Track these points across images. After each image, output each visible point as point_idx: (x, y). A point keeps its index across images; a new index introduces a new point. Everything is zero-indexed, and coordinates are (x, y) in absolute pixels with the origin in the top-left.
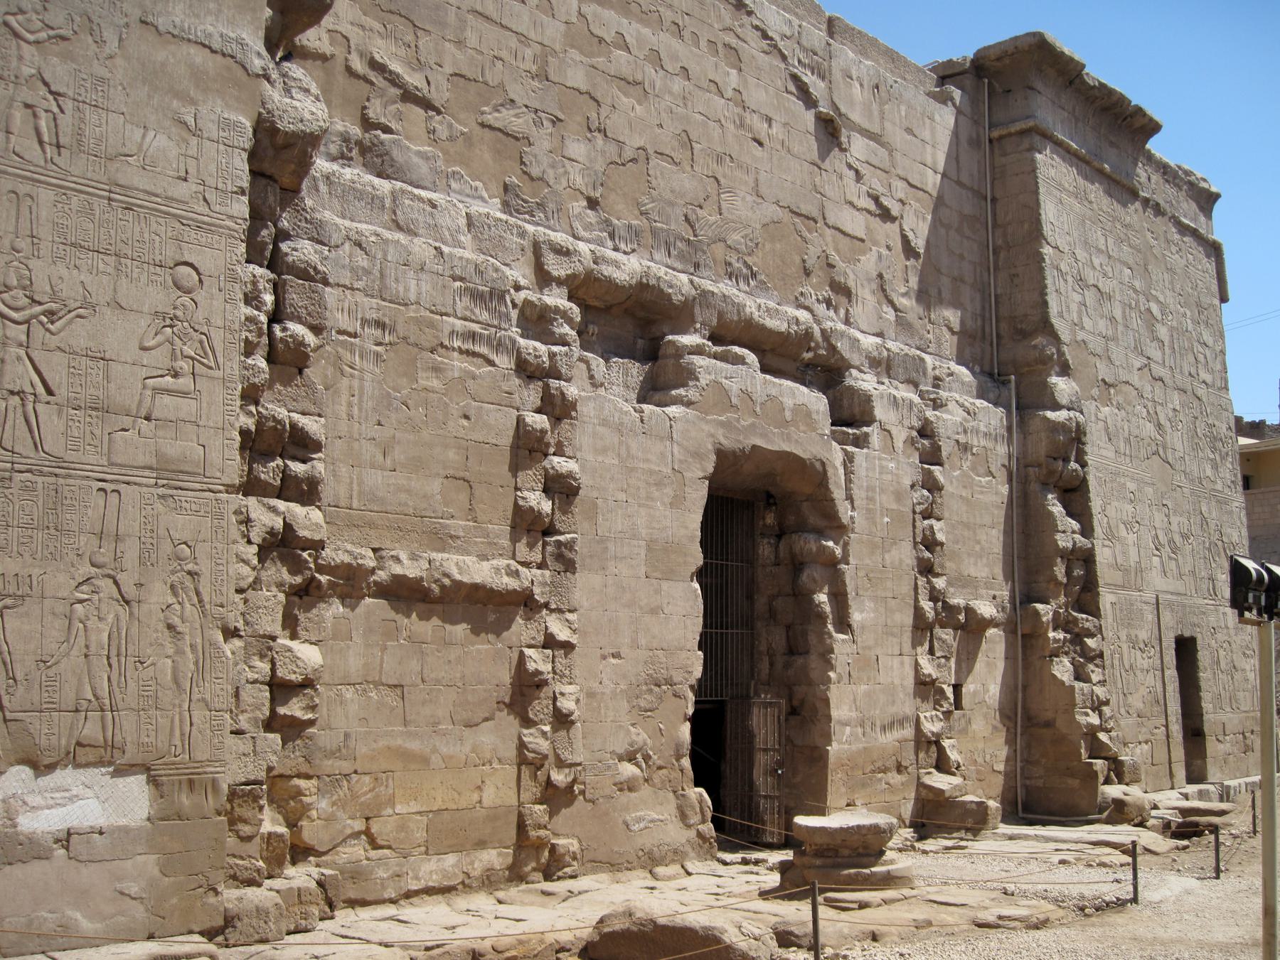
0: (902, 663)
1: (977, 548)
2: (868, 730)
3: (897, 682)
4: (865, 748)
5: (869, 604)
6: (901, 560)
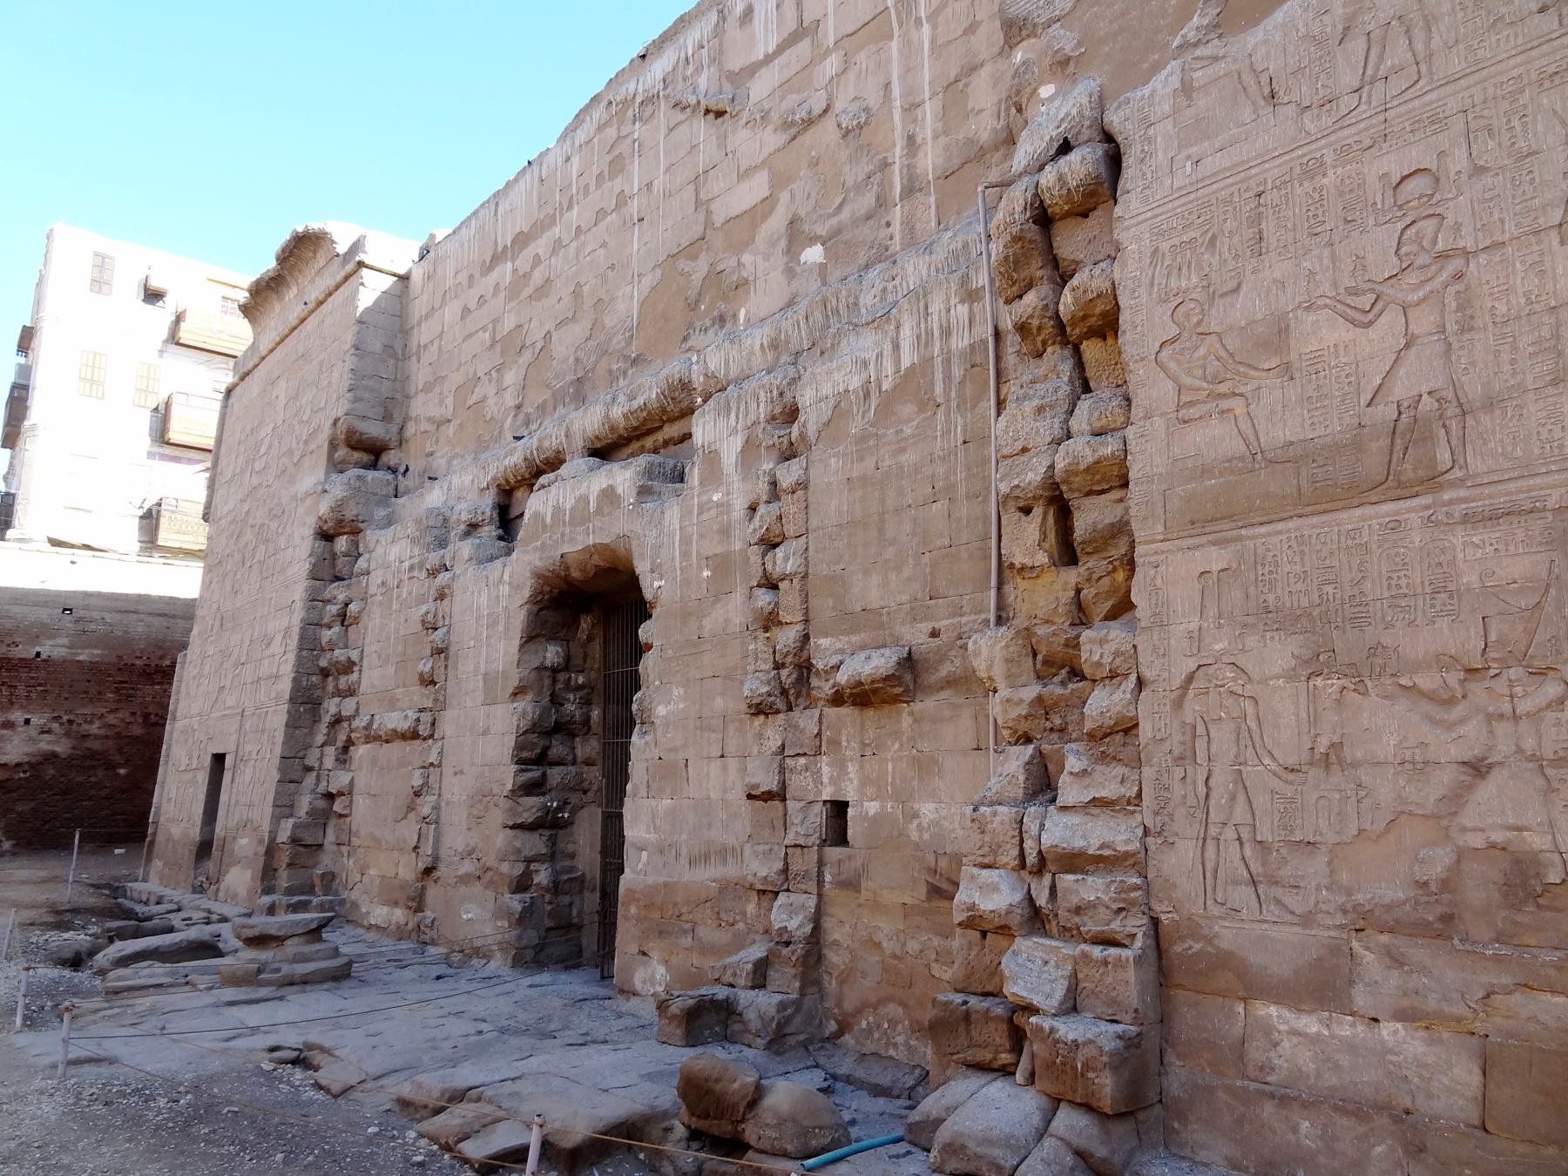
0: (725, 768)
1: (890, 552)
2: (672, 859)
3: (713, 795)
4: (666, 885)
5: (677, 691)
6: (727, 621)
